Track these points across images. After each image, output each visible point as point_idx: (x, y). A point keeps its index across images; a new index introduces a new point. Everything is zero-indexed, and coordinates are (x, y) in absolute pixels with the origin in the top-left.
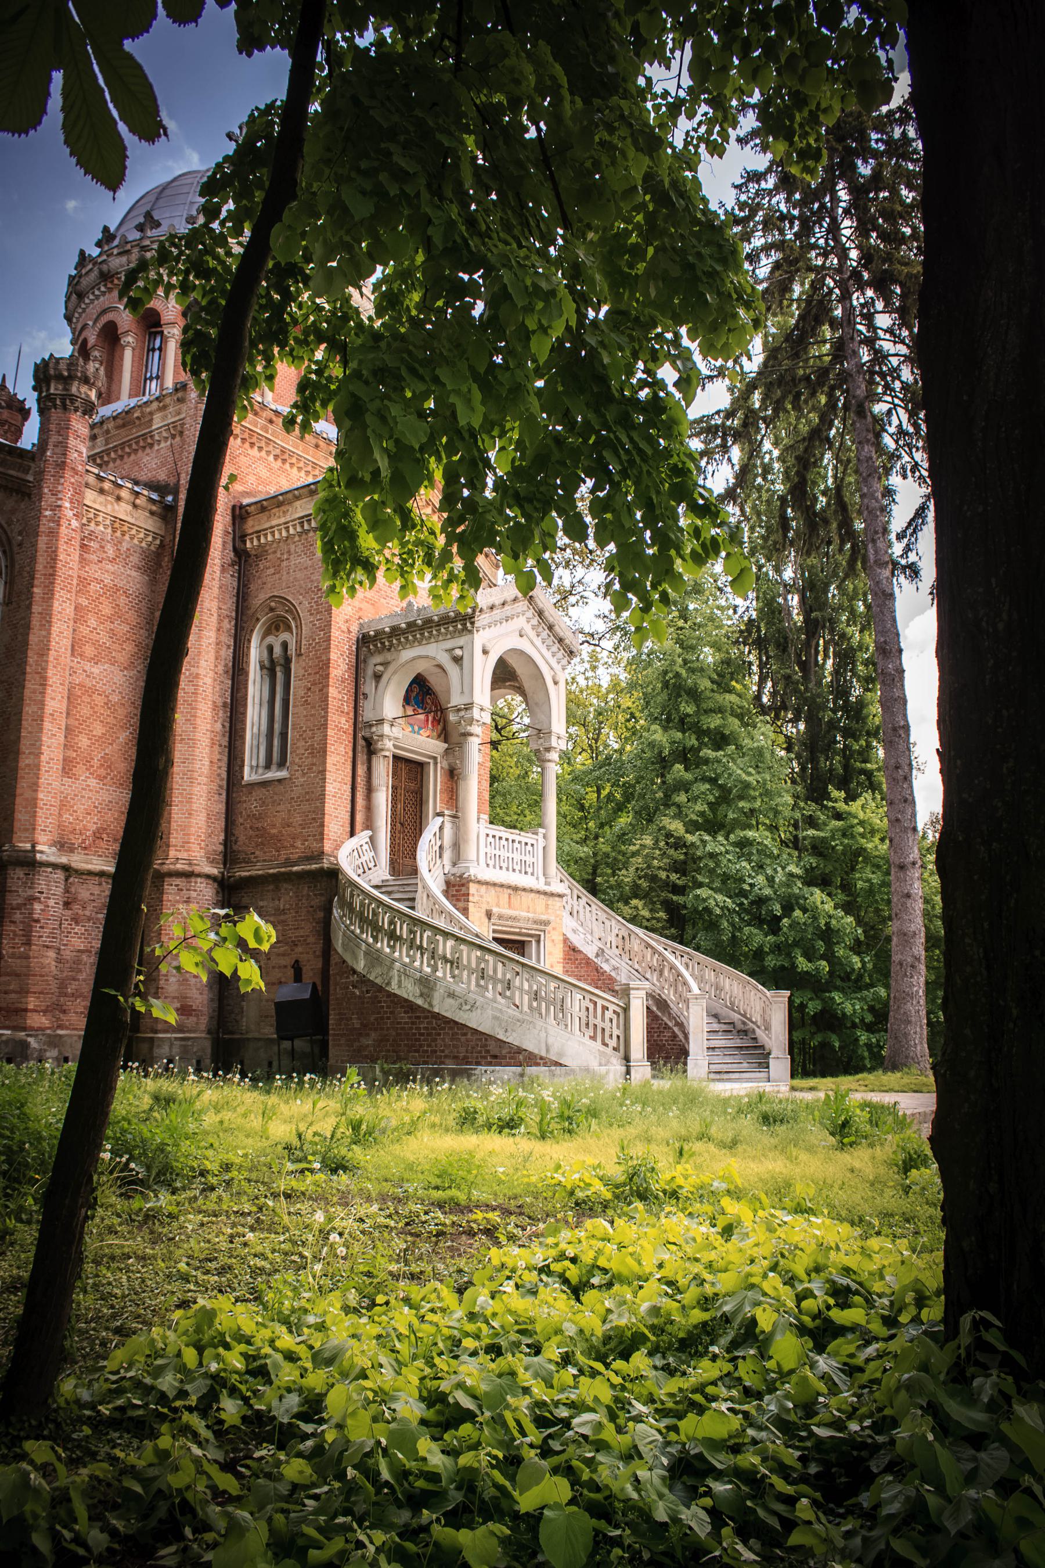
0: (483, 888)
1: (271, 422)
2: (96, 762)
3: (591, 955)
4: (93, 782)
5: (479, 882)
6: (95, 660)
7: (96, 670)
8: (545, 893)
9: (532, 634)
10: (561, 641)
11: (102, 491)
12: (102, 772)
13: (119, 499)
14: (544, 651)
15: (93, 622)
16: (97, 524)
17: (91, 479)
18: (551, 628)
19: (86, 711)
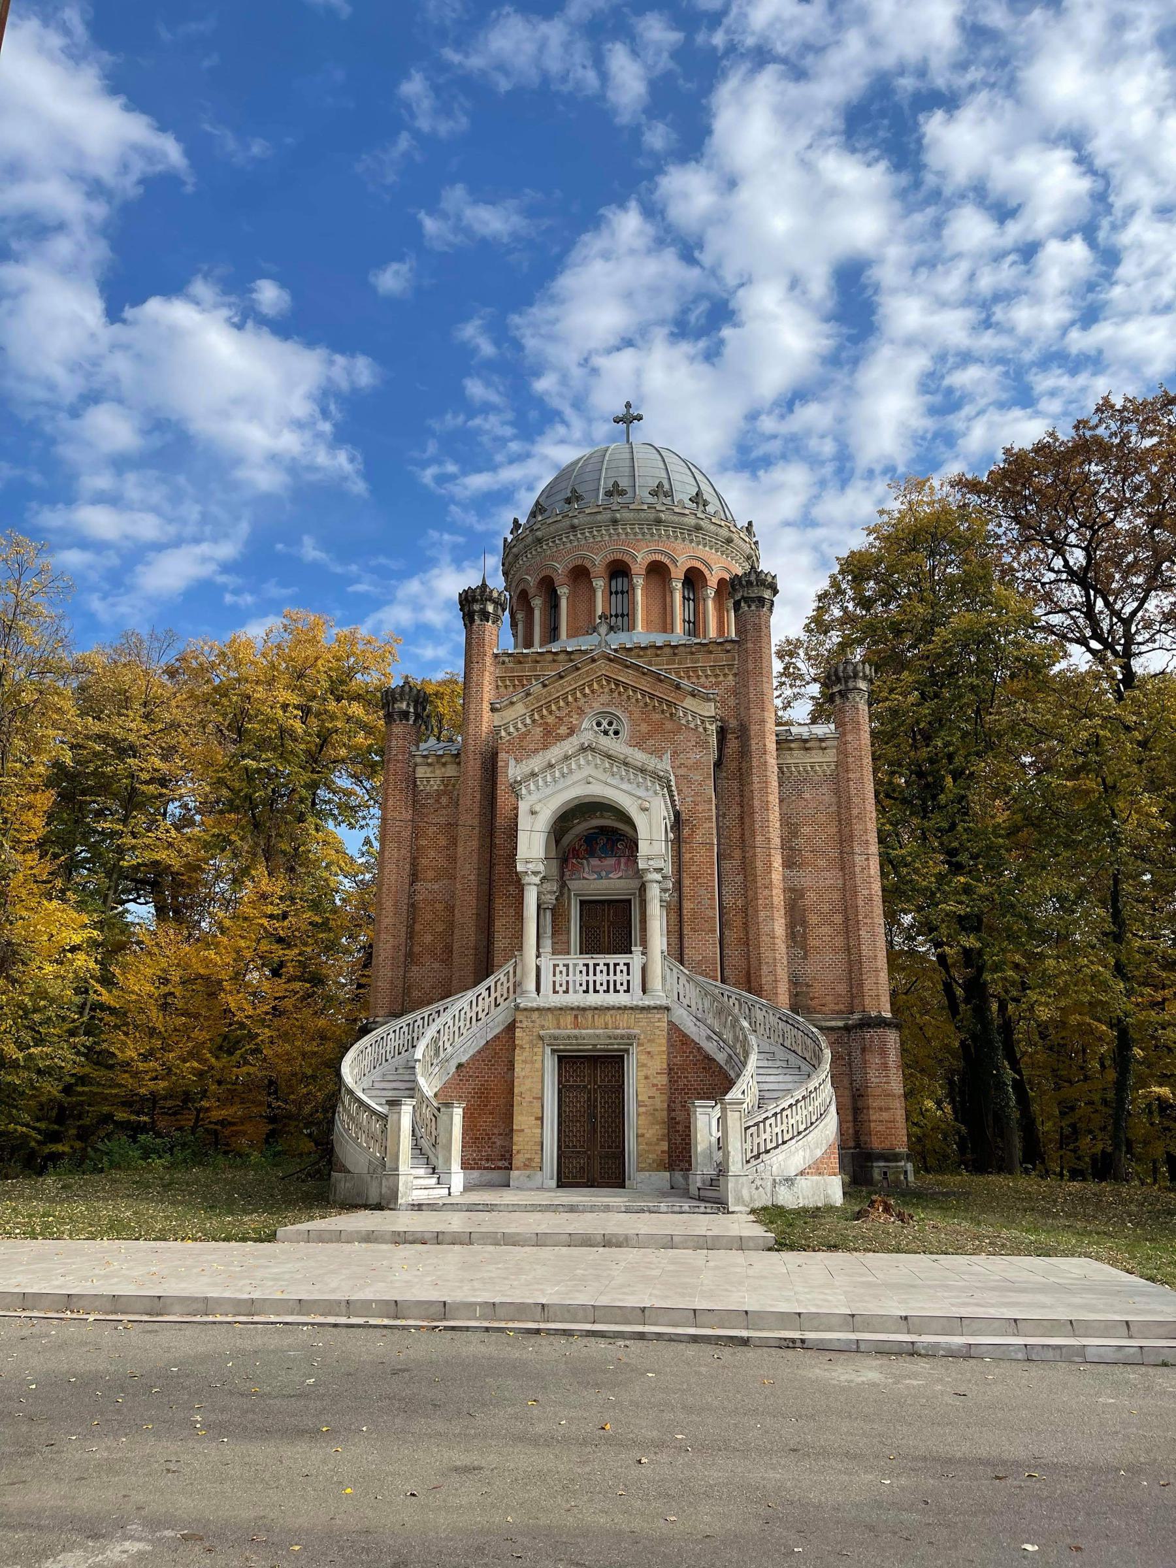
0: (535, 1015)
1: (537, 662)
2: (439, 951)
3: (722, 1063)
4: (436, 965)
5: (525, 1009)
6: (436, 880)
7: (436, 887)
8: (643, 1009)
9: (603, 777)
10: (642, 771)
11: (429, 765)
12: (445, 956)
13: (444, 764)
14: (625, 786)
15: (432, 854)
16: (432, 786)
17: (419, 760)
18: (626, 764)
19: (429, 917)
